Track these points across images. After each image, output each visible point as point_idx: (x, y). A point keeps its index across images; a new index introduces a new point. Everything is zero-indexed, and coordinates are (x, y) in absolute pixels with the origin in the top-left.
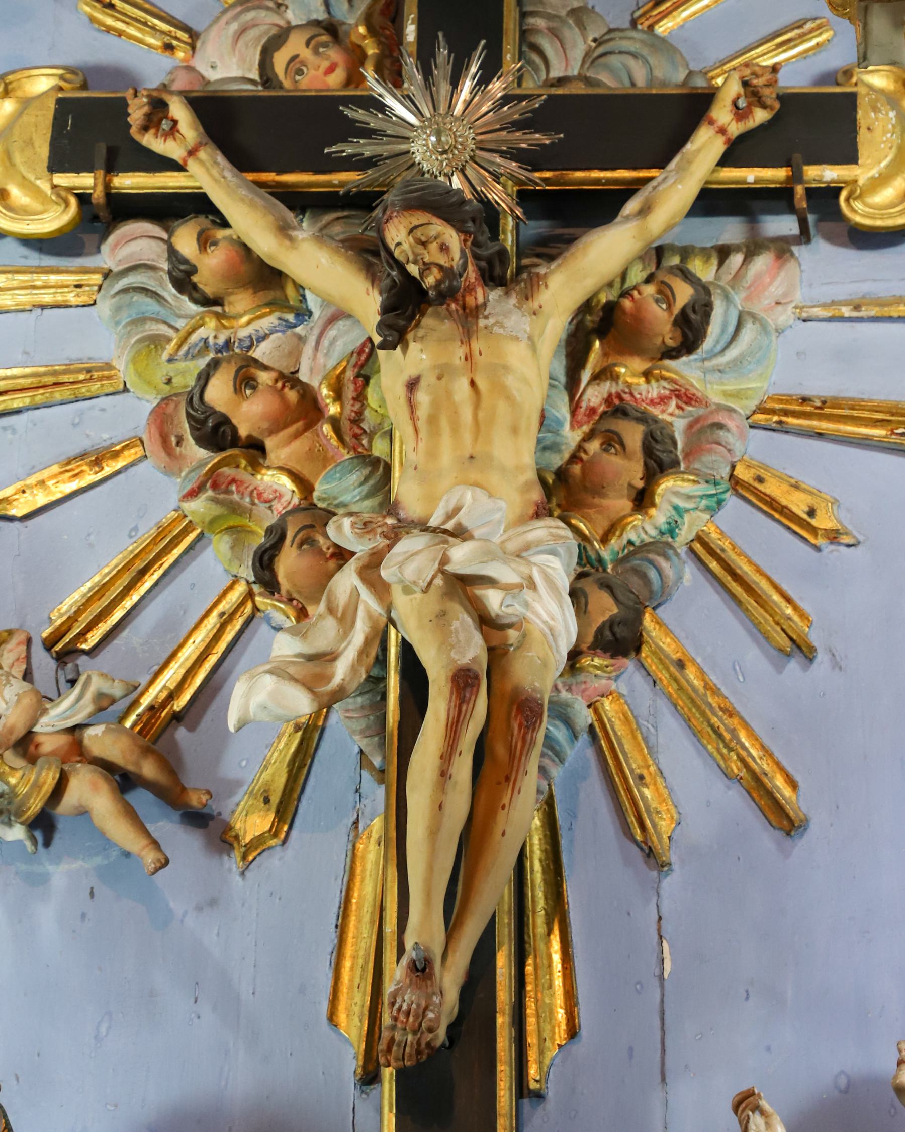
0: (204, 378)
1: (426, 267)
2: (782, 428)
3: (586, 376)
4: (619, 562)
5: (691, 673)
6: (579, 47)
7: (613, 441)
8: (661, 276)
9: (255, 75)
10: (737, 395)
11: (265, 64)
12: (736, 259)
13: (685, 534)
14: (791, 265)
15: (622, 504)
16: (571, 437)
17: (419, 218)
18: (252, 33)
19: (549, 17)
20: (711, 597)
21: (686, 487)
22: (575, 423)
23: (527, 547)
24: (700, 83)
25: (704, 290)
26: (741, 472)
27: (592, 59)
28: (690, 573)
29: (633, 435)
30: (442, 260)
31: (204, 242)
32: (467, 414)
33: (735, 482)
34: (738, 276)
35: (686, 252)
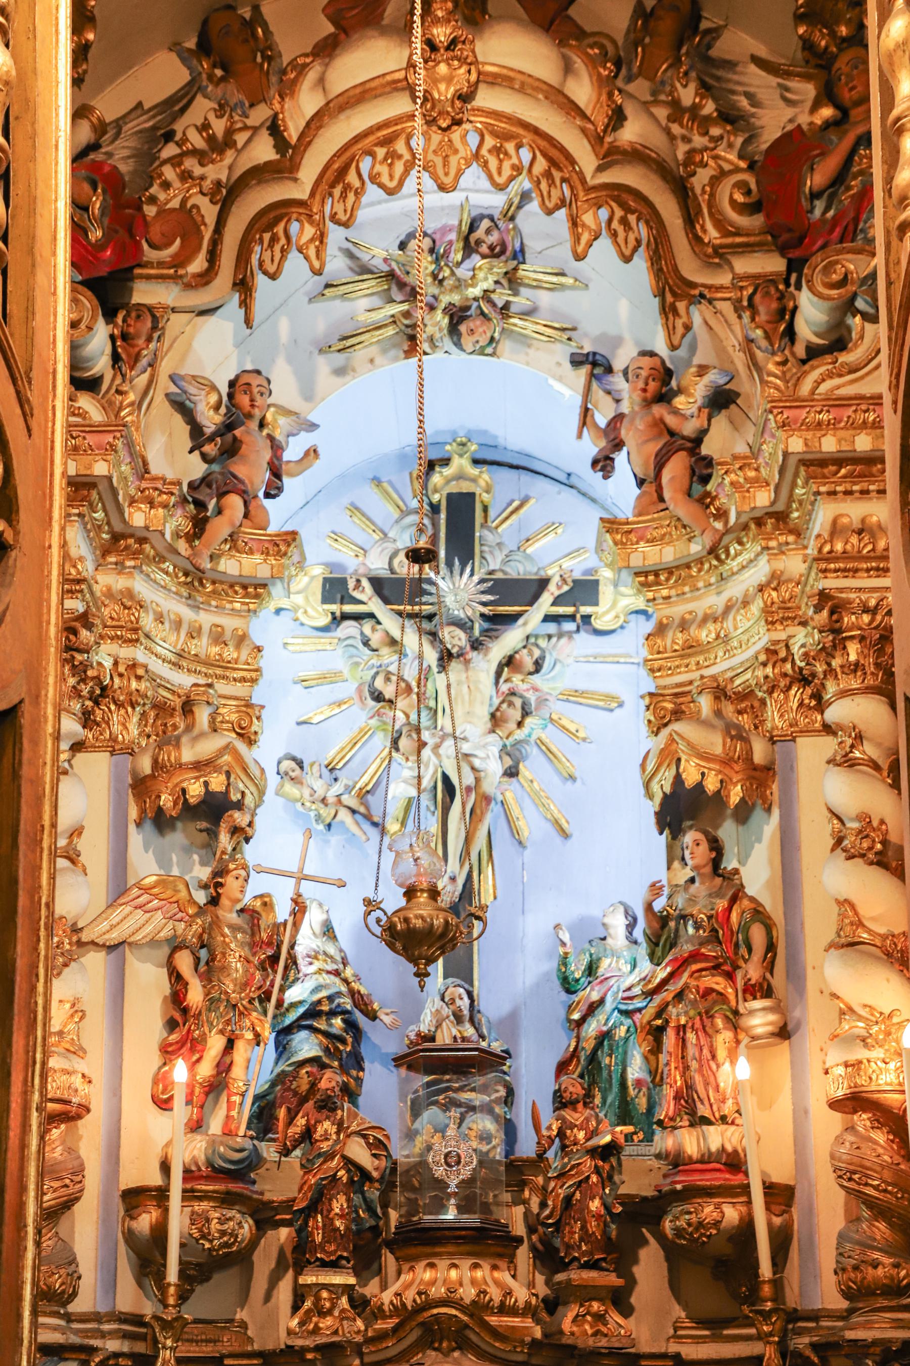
0: (374, 678)
1: (454, 646)
2: (568, 701)
3: (502, 680)
4: (513, 746)
5: (535, 784)
6: (500, 556)
7: (511, 704)
8: (529, 646)
9: (387, 567)
10: (553, 689)
11: (390, 563)
12: (554, 640)
13: (534, 737)
14: (573, 642)
15: (512, 725)
16: (496, 702)
17: (452, 628)
18: (386, 552)
19: (490, 546)
20: (542, 759)
21: (535, 721)
22: (498, 697)
23: (486, 744)
24: (542, 574)
25: (543, 651)
26: (554, 717)
27: (505, 562)
28: (535, 750)
29: (518, 702)
30: (459, 643)
31: (373, 630)
32: (467, 697)
33: (551, 719)
34: (555, 646)
35: (537, 637)
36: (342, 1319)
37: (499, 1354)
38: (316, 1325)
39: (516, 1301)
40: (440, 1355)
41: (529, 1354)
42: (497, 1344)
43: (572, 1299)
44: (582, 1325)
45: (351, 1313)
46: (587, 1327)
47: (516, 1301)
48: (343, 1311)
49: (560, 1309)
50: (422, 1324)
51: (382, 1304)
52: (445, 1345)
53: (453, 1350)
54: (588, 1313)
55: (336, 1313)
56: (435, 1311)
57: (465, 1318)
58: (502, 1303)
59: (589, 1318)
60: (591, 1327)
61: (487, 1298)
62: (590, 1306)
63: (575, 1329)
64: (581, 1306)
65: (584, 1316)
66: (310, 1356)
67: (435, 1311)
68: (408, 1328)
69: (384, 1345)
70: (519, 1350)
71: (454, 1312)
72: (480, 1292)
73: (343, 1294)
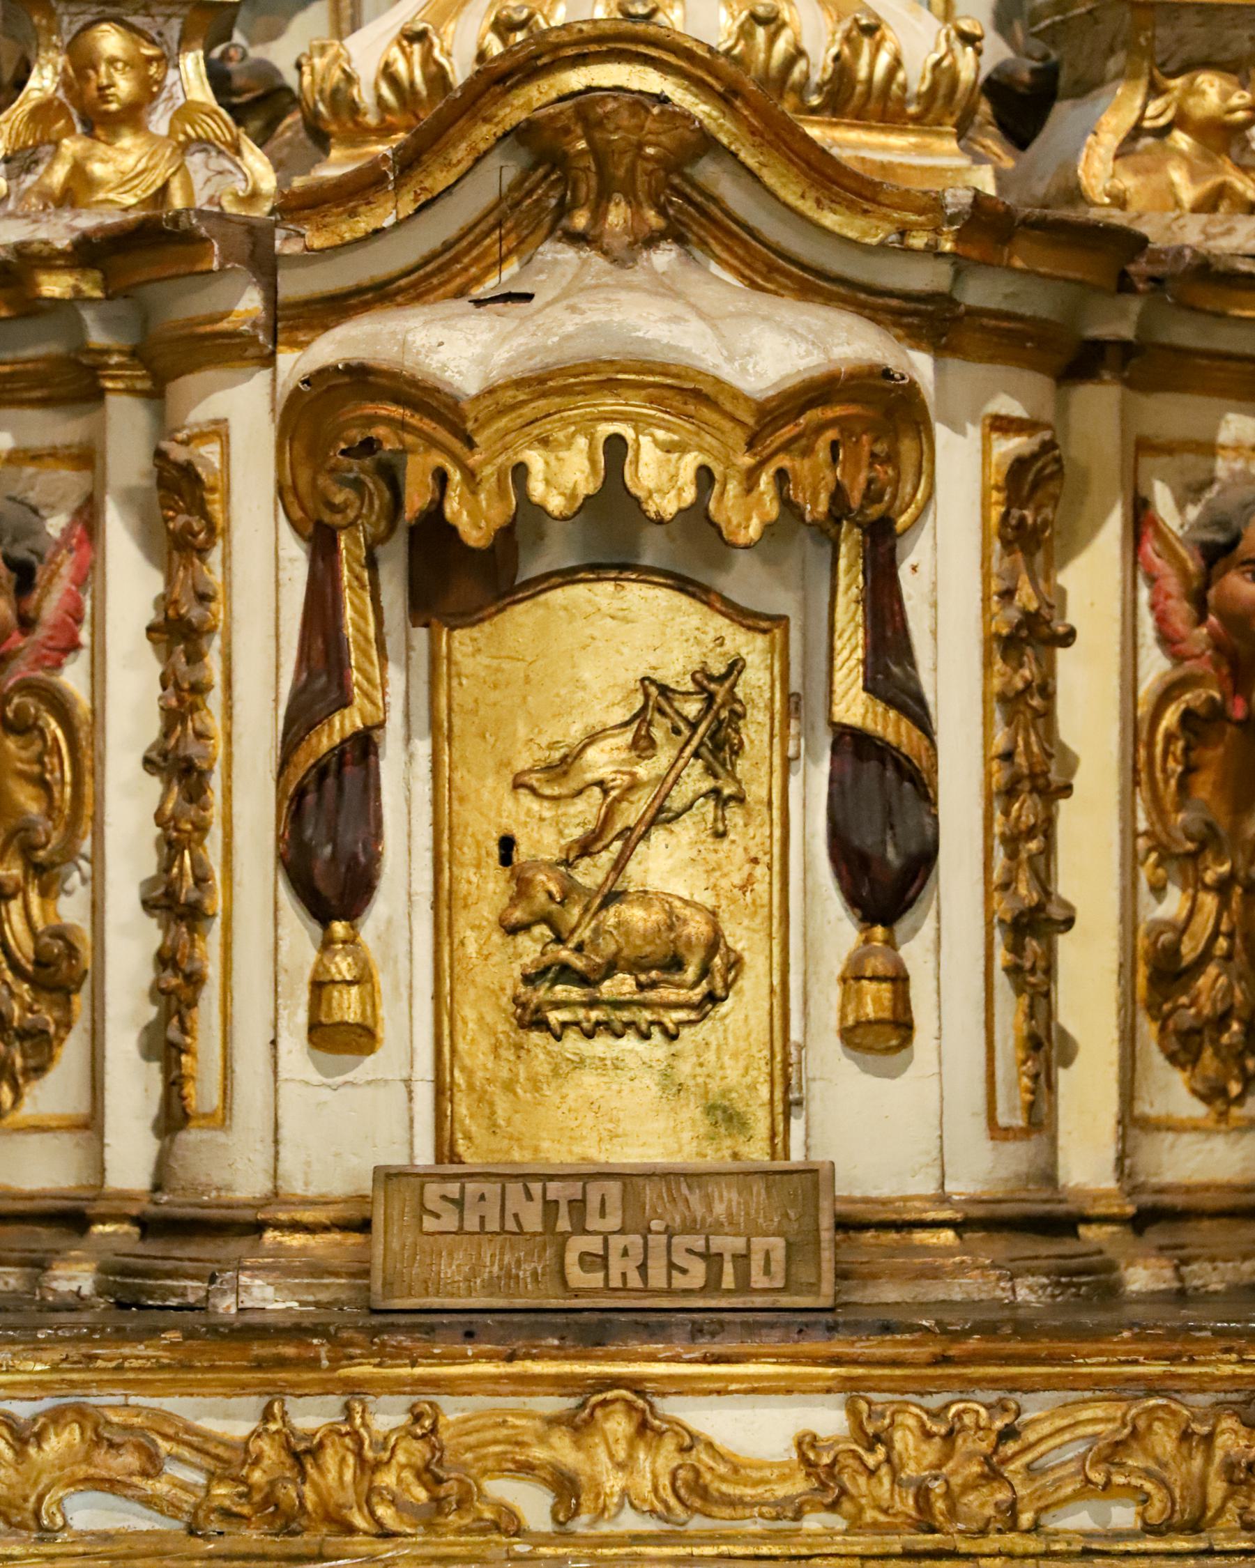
36: (185, 148)
37: (836, 262)
38: (78, 170)
39: (897, 64)
40: (598, 262)
41: (960, 265)
42: (829, 220)
43: (1113, 65)
44: (1158, 167)
45: (220, 125)
46: (1178, 175)
47: (897, 64)
48: (187, 112)
49: (1064, 114)
50: (523, 134)
51: (349, 79)
52: (617, 215)
53: (652, 241)
54: (1181, 121)
55: (159, 122)
56: (576, 79)
57: (701, 109)
58: (842, 70)
59: (1181, 140)
60: (1194, 177)
61: (782, 46)
62: (1191, 90)
63: (1128, 182)
64: (1155, 90)
65: (1162, 133)
66: (54, 286)
67: (576, 79)
68: (461, 154)
69: (363, 225)
70: (918, 241)
71: (650, 80)
72: (755, 18)
73: (185, 42)
